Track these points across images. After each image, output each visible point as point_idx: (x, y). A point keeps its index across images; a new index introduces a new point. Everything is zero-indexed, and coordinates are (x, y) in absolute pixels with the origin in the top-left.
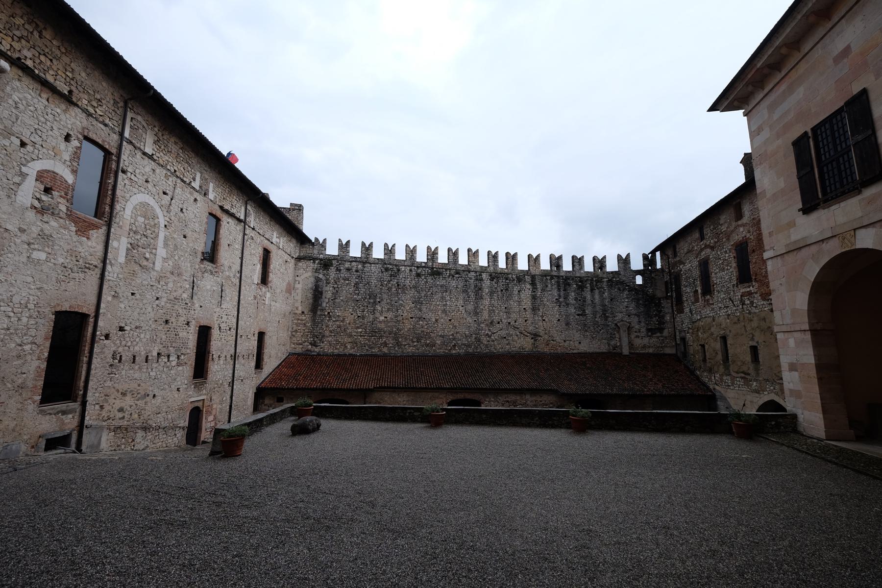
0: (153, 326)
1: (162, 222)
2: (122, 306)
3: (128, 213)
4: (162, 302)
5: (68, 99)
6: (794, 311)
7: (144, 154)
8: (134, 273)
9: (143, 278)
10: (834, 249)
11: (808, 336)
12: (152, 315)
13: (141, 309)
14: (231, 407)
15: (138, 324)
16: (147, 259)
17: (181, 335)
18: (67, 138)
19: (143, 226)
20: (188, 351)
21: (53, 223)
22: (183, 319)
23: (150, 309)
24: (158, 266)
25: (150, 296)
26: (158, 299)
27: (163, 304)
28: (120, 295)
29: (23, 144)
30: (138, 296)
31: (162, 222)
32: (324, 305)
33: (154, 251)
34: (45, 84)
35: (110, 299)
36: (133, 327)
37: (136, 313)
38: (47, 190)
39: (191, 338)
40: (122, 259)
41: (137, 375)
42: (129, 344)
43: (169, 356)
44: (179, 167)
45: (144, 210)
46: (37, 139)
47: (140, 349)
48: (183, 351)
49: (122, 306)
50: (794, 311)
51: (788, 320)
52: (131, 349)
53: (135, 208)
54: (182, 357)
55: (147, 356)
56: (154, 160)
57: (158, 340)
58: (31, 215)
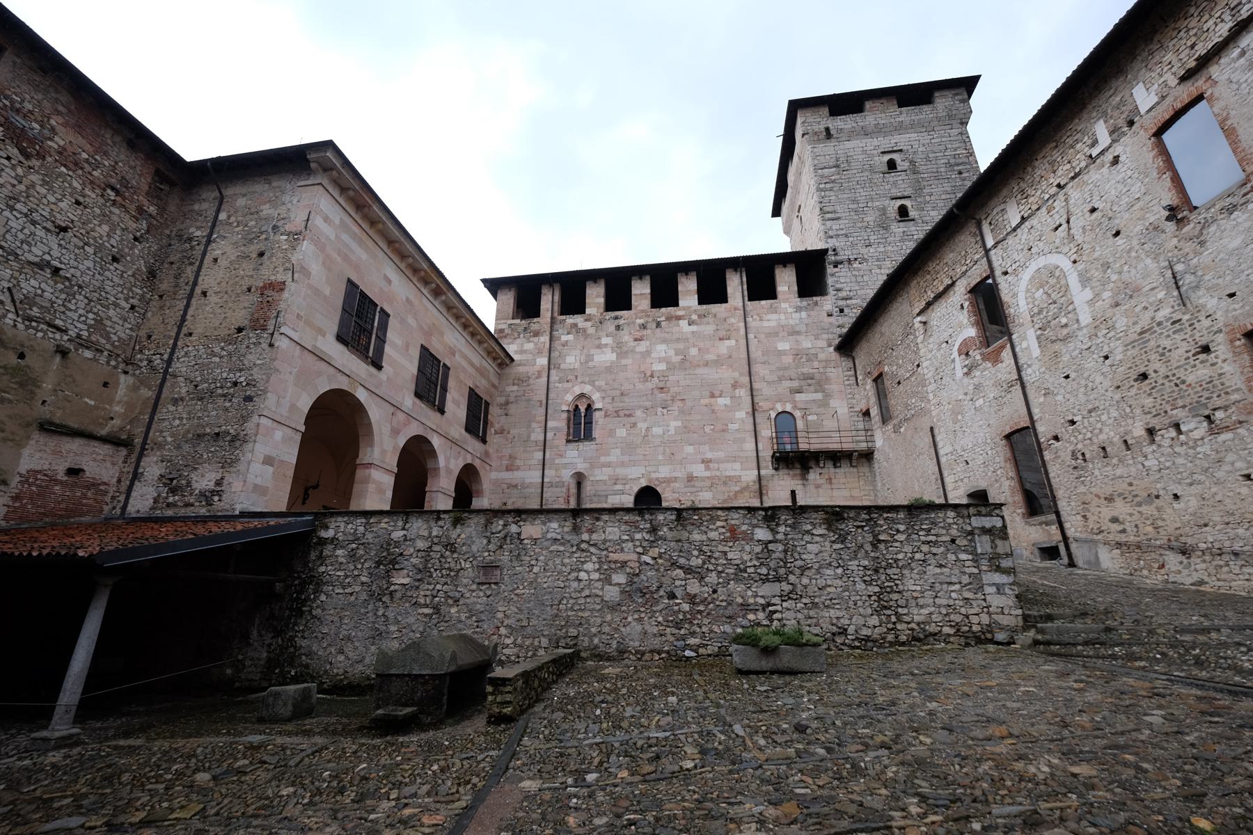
0: (1117, 396)
1: (1064, 263)
2: (1059, 398)
3: (1022, 303)
4: (1118, 356)
5: (953, 283)
6: (293, 407)
7: (1014, 230)
8: (1057, 355)
9: (1068, 352)
10: (342, 383)
11: (298, 437)
12: (1107, 383)
13: (1086, 386)
15: (1090, 407)
16: (1066, 325)
17: (1191, 379)
18: (962, 307)
20: (1236, 397)
21: (978, 373)
22: (1181, 351)
23: (1099, 379)
24: (1085, 318)
25: (1092, 363)
26: (1106, 357)
27: (1119, 357)
31: (1064, 263)
33: (1070, 308)
34: (939, 297)
35: (1042, 399)
36: (1085, 413)
37: (1080, 396)
40: (1036, 352)
41: (1119, 472)
42: (1089, 435)
43: (1177, 426)
45: (1039, 281)
47: (1110, 435)
48: (1219, 403)
50: (293, 407)
51: (284, 411)
52: (1095, 440)
53: (1028, 291)
54: (1219, 415)
55: (1125, 441)
57: (1138, 411)
58: (966, 380)
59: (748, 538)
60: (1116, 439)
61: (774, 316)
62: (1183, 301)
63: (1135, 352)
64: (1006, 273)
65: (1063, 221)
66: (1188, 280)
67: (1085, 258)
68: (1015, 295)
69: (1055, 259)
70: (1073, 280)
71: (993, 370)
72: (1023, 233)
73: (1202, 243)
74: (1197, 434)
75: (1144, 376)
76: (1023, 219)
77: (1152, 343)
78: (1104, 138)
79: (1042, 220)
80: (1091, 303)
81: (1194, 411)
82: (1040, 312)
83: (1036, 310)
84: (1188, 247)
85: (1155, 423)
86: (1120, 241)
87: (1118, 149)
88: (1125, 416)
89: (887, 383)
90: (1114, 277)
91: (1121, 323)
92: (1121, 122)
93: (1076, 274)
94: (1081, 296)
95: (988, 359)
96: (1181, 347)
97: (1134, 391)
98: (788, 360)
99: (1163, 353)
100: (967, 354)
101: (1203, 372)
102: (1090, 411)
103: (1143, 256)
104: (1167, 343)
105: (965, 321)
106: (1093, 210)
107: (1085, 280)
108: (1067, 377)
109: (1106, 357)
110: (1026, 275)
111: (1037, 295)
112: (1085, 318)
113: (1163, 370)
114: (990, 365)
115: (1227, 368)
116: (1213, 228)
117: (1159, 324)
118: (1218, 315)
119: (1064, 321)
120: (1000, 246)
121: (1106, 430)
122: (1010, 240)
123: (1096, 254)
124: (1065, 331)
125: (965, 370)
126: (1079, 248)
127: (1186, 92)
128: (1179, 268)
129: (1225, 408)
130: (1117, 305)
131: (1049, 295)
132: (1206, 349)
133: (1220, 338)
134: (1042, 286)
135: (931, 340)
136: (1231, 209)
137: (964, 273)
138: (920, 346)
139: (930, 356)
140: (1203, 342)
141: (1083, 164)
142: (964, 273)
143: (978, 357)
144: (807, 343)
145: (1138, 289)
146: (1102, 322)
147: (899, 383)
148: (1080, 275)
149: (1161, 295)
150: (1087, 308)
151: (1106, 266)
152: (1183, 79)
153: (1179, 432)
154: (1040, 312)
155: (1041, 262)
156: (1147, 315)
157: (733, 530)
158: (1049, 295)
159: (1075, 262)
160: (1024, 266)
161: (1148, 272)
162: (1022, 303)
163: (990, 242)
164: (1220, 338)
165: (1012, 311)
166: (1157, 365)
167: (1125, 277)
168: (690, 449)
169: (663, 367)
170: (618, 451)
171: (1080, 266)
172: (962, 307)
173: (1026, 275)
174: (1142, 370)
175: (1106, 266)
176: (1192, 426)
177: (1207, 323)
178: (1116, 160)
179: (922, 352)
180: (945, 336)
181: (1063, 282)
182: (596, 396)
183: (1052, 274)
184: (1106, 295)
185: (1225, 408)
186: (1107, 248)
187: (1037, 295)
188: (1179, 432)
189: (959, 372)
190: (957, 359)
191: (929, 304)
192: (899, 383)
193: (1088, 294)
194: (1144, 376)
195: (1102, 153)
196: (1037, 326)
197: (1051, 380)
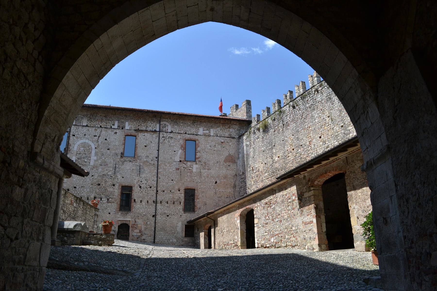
0: (91, 186)
1: (93, 147)
3: (75, 148)
7: (83, 126)
12: (90, 182)
14: (155, 228)
16: (86, 162)
17: (108, 190)
20: (115, 197)
22: (109, 183)
24: (92, 163)
26: (93, 176)
27: (96, 177)
31: (93, 147)
32: (250, 163)
33: (89, 158)
39: (117, 191)
44: (103, 124)
45: (84, 145)
48: (111, 196)
49: (75, 180)
52: (80, 194)
53: (79, 145)
54: (110, 199)
55: (88, 198)
56: (88, 126)
57: (94, 192)
59: (73, 205)
60: (86, 196)
62: (115, 173)
63: (100, 178)
64: (74, 135)
65: (98, 135)
66: (117, 169)
69: (90, 143)
70: (93, 152)
72: (85, 129)
73: (123, 164)
74: (104, 202)
75: (99, 185)
76: (87, 126)
77: (104, 178)
78: (116, 126)
79: (92, 130)
80: (95, 161)
81: (106, 196)
82: (79, 154)
83: (79, 152)
84: (121, 163)
85: (97, 196)
86: (108, 151)
87: (117, 131)
88: (90, 192)
90: (103, 158)
91: (100, 170)
92: (121, 126)
93: (94, 151)
94: (93, 158)
96: (110, 183)
97: (95, 187)
99: (106, 182)
101: (111, 190)
102: (82, 187)
104: (107, 180)
106: (106, 139)
107: (96, 154)
110: (81, 141)
112: (92, 163)
113: (104, 185)
115: (116, 191)
118: (119, 180)
119: (86, 160)
120: (76, 126)
121: (84, 193)
122: (80, 128)
124: (85, 163)
127: (134, 133)
128: (117, 166)
129: (112, 198)
130: (101, 165)
131: (85, 151)
132: (114, 185)
133: (117, 184)
134: (84, 148)
136: (130, 161)
140: (114, 183)
141: (109, 127)
145: (107, 165)
148: (96, 152)
149: (111, 169)
150: (93, 161)
151: (103, 155)
152: (135, 130)
153: (101, 200)
155: (87, 141)
156: (107, 172)
157: (71, 201)
158: (85, 151)
161: (111, 162)
162: (75, 148)
164: (117, 184)
165: (71, 147)
166: (103, 184)
167: (106, 160)
171: (97, 150)
173: (81, 141)
174: (100, 183)
175: (103, 155)
176: (104, 199)
177: (117, 180)
178: (116, 133)
181: (90, 151)
183: (88, 147)
184: (100, 161)
185: (112, 198)
186: (105, 151)
188: (101, 200)
193: (95, 158)
194: (99, 185)
195: (114, 129)
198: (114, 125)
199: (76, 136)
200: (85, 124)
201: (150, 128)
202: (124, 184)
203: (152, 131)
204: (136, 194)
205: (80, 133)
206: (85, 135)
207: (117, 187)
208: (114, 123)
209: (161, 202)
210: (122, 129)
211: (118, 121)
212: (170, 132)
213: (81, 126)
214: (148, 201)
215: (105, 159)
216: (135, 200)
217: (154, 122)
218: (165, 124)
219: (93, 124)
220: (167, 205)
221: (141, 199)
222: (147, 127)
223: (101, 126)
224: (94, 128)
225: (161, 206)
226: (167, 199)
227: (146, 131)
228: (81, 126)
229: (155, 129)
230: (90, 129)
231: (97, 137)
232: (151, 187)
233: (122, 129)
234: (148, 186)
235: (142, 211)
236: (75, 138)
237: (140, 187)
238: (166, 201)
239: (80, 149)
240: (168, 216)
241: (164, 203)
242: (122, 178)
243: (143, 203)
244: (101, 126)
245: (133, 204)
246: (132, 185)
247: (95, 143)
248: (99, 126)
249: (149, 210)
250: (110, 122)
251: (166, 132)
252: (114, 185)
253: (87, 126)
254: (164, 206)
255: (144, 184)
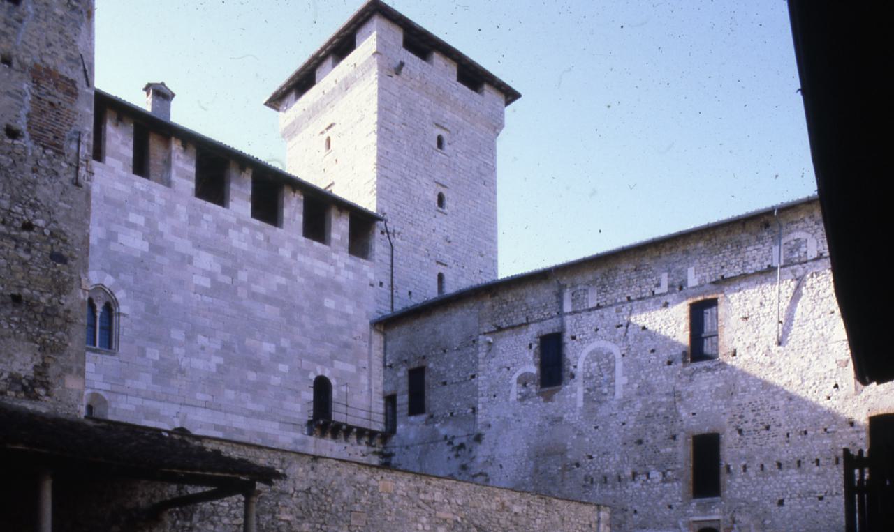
1: (618, 354)
3: (580, 366)
5: (527, 324)
7: (590, 310)
8: (594, 411)
18: (530, 346)
19: (597, 368)
21: (530, 403)
24: (619, 394)
26: (624, 424)
27: (631, 426)
28: (584, 432)
29: (509, 368)
30: (601, 428)
31: (618, 354)
33: (612, 384)
34: (513, 327)
38: (525, 385)
40: (580, 404)
46: (515, 360)
53: (586, 359)
58: (518, 404)
61: (326, 266)
63: (640, 426)
64: (574, 338)
67: (630, 356)
68: (577, 358)
70: (619, 366)
71: (544, 405)
72: (594, 317)
73: (691, 380)
76: (598, 307)
77: (651, 425)
82: (590, 378)
83: (588, 375)
89: (428, 378)
90: (643, 377)
94: (621, 380)
95: (542, 396)
98: (332, 320)
99: (654, 432)
100: (525, 385)
103: (662, 372)
105: (531, 358)
108: (596, 428)
109: (624, 424)
110: (589, 348)
111: (592, 365)
112: (619, 394)
114: (541, 400)
116: (698, 375)
117: (658, 415)
118: (685, 422)
120: (575, 315)
122: (584, 316)
123: (638, 357)
125: (519, 396)
126: (628, 349)
131: (600, 369)
134: (598, 361)
135: (494, 360)
137: (541, 320)
138: (480, 361)
139: (488, 373)
140: (674, 433)
142: (541, 320)
143: (534, 391)
144: (349, 309)
146: (626, 402)
147: (444, 383)
148: (624, 365)
154: (590, 378)
158: (600, 369)
159: (623, 355)
160: (589, 341)
163: (568, 307)
164: (683, 433)
167: (649, 379)
168: (230, 394)
169: (206, 283)
170: (149, 377)
171: (627, 361)
172: (530, 346)
173: (589, 348)
177: (679, 424)
179: (481, 366)
180: (508, 363)
181: (612, 365)
182: (120, 295)
184: (636, 385)
187: (592, 365)
189: (514, 396)
190: (515, 385)
191: (500, 329)
192: (444, 383)
193: (625, 380)
196: (586, 386)
197: (585, 426)
198: (658, 285)
199: (577, 338)
200: (592, 304)
201: (754, 266)
202: (697, 432)
203: (761, 273)
204: (730, 452)
205: (585, 329)
206: (597, 330)
207: (680, 439)
208: (660, 280)
209: (799, 462)
210: (681, 288)
211: (669, 271)
212: (816, 259)
213: (584, 310)
214: (762, 466)
215: (647, 376)
216: (728, 467)
217: (763, 244)
218: (799, 239)
219: (619, 294)
220: (816, 469)
221: (743, 463)
222: (745, 263)
223: (629, 298)
224: (614, 308)
225: (801, 473)
226: (816, 455)
227: (744, 277)
228: (584, 310)
229: (769, 263)
230: (606, 314)
231: (624, 328)
232: (768, 428)
233: (681, 288)
234: (762, 427)
235: (748, 493)
236: (576, 344)
237: (740, 431)
238: (814, 458)
239: (589, 367)
240: (821, 498)
241: (808, 465)
242: (691, 416)
243: (751, 473)
244: (629, 298)
245: (725, 479)
246: (718, 430)
247: (621, 344)
248: (625, 299)
249: (767, 488)
250: (649, 280)
251: (800, 263)
252: (674, 438)
253: (598, 307)
254: (810, 471)
255: (750, 423)
